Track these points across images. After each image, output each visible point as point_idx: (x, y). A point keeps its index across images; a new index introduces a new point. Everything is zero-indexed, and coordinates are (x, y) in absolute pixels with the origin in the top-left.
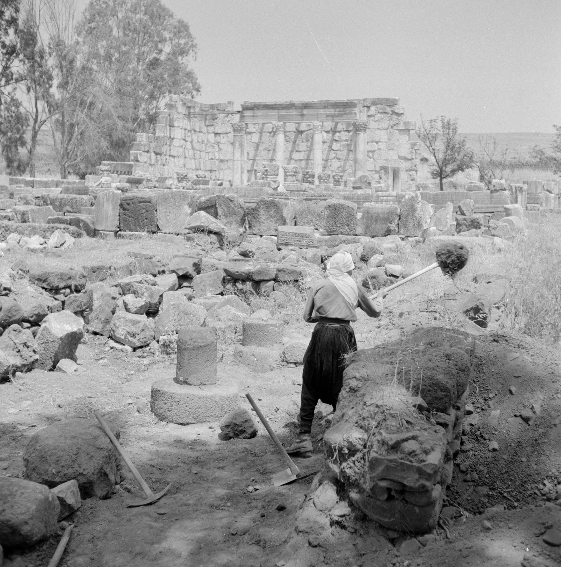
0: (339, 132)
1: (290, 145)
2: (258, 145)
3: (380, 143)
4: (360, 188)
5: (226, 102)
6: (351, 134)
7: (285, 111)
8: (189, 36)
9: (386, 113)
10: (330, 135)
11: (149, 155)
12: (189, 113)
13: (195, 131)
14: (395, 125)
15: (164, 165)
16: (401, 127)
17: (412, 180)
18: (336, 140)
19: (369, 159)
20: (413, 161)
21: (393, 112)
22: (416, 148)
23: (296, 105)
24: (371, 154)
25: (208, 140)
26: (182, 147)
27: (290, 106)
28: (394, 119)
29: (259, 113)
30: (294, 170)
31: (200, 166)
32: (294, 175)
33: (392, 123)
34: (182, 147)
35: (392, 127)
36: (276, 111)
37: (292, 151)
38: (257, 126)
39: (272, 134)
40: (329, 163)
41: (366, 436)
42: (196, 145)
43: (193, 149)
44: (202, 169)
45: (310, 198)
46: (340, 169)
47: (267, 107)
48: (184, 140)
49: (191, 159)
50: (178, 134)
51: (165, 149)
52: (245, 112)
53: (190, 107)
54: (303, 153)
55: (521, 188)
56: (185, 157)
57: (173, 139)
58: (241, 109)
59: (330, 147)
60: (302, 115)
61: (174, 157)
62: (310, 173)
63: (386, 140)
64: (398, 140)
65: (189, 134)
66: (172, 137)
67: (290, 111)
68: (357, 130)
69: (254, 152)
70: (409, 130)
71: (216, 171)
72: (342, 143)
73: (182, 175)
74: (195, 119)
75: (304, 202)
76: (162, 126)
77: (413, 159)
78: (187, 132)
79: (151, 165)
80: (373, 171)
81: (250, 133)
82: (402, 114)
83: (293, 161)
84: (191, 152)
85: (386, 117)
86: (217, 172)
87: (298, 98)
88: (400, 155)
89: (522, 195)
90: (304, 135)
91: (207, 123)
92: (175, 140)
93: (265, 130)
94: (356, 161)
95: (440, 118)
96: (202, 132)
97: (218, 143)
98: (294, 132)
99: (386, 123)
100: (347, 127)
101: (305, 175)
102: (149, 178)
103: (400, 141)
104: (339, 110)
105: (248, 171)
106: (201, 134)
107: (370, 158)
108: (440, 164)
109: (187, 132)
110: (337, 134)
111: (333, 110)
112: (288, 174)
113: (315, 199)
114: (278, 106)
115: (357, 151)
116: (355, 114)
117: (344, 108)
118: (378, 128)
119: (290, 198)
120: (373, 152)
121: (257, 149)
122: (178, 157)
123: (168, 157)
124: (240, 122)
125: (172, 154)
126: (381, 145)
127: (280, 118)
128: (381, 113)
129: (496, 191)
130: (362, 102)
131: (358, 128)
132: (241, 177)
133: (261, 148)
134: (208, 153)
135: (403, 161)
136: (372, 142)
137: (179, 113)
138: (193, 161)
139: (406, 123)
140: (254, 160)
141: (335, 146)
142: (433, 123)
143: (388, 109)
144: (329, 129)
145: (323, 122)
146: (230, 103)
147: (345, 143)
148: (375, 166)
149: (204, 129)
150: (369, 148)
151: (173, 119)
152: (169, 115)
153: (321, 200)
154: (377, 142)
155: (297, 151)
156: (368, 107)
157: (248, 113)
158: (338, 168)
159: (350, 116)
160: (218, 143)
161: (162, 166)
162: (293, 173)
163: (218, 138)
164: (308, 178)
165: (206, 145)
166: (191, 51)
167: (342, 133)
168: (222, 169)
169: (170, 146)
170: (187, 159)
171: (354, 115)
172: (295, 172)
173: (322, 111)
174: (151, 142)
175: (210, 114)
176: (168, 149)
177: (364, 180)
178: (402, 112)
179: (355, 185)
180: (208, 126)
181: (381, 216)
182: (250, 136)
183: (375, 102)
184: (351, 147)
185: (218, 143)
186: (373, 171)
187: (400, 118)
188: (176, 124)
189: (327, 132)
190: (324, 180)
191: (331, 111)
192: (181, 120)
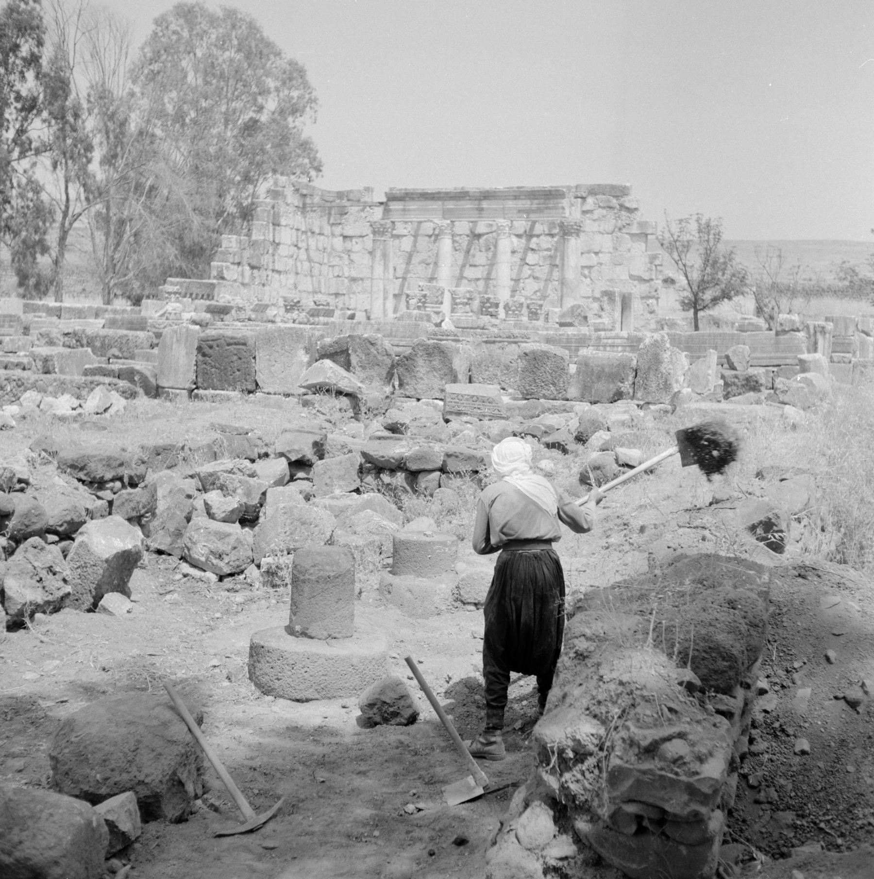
0: (538, 236)
1: (460, 256)
2: (410, 256)
3: (600, 255)
4: (570, 325)
5: (361, 188)
6: (555, 239)
7: (452, 202)
8: (306, 85)
9: (610, 208)
10: (523, 241)
11: (240, 269)
12: (304, 205)
13: (313, 233)
14: (624, 227)
15: (264, 285)
16: (635, 230)
17: (651, 312)
18: (532, 250)
19: (584, 279)
20: (652, 283)
21: (622, 206)
22: (657, 262)
23: (471, 194)
24: (586, 272)
25: (332, 246)
26: (292, 256)
27: (461, 195)
28: (624, 218)
29: (413, 205)
30: (468, 295)
31: (320, 287)
32: (467, 304)
33: (620, 223)
34: (292, 256)
35: (620, 229)
36: (440, 203)
37: (464, 266)
38: (409, 227)
39: (433, 238)
40: (521, 285)
41: (602, 731)
43: (309, 260)
44: (323, 291)
45: (493, 339)
46: (538, 294)
47: (426, 196)
48: (296, 246)
49: (306, 276)
50: (286, 236)
51: (266, 260)
52: (390, 203)
53: (305, 196)
54: (481, 268)
55: (823, 328)
56: (297, 274)
57: (278, 244)
58: (384, 200)
59: (523, 259)
60: (481, 210)
61: (279, 272)
62: (491, 301)
63: (611, 250)
64: (629, 250)
65: (304, 237)
66: (277, 241)
67: (460, 203)
68: (565, 234)
69: (404, 266)
70: (646, 235)
71: (344, 294)
72: (541, 254)
73: (292, 301)
74: (314, 214)
75: (484, 345)
76: (262, 225)
77: (652, 280)
78: (300, 233)
79: (243, 284)
80: (589, 298)
81: (398, 237)
82: (636, 209)
83: (465, 281)
84: (306, 265)
85: (611, 214)
86: (346, 297)
87: (474, 183)
88: (633, 273)
89: (824, 338)
90: (482, 240)
91: (332, 221)
92: (281, 246)
93: (421, 232)
94: (563, 282)
95: (695, 217)
96: (323, 234)
97: (349, 252)
98: (468, 236)
99: (610, 225)
100: (550, 229)
101: (484, 303)
102: (241, 306)
103: (633, 251)
104: (536, 202)
105: (395, 296)
106: (322, 238)
107: (586, 277)
108: (695, 288)
109: (300, 233)
110: (534, 240)
111: (529, 202)
112: (458, 301)
113: (500, 342)
114: (442, 195)
115: (566, 267)
116: (563, 208)
117: (545, 200)
118: (597, 230)
119: (461, 339)
120: (590, 267)
121: (408, 263)
122: (286, 272)
123: (270, 273)
124: (383, 219)
125: (276, 268)
126: (604, 258)
127: (446, 213)
128: (604, 208)
129: (785, 332)
130: (574, 190)
131: (567, 231)
132: (384, 305)
133: (415, 260)
134: (333, 266)
135: (636, 282)
136: (589, 252)
137: (288, 205)
138: (309, 278)
139: (642, 225)
140: (404, 279)
141: (531, 258)
142: (684, 224)
143: (614, 202)
144: (521, 232)
145: (512, 221)
146: (368, 189)
147: (546, 253)
148: (593, 291)
149: (327, 230)
150: (584, 261)
151: (279, 213)
152: (273, 207)
153: (510, 343)
154: (596, 253)
155: (471, 266)
156: (584, 198)
157: (395, 206)
158: (535, 292)
159: (554, 211)
160: (349, 251)
161: (261, 287)
162: (466, 300)
163: (348, 244)
164: (489, 307)
165: (330, 255)
166: (308, 109)
167: (542, 237)
168: (354, 293)
169: (273, 255)
170: (299, 276)
171: (561, 211)
172: (470, 299)
173: (510, 204)
174: (244, 249)
175: (337, 206)
176: (271, 260)
177: (577, 313)
178: (634, 206)
179: (563, 321)
180: (333, 224)
181: (607, 370)
182: (397, 241)
183: (593, 191)
184: (556, 261)
185: (349, 252)
186: (589, 298)
187: (633, 215)
188: (283, 222)
189: (519, 236)
190: (514, 311)
191: (526, 204)
192: (291, 215)
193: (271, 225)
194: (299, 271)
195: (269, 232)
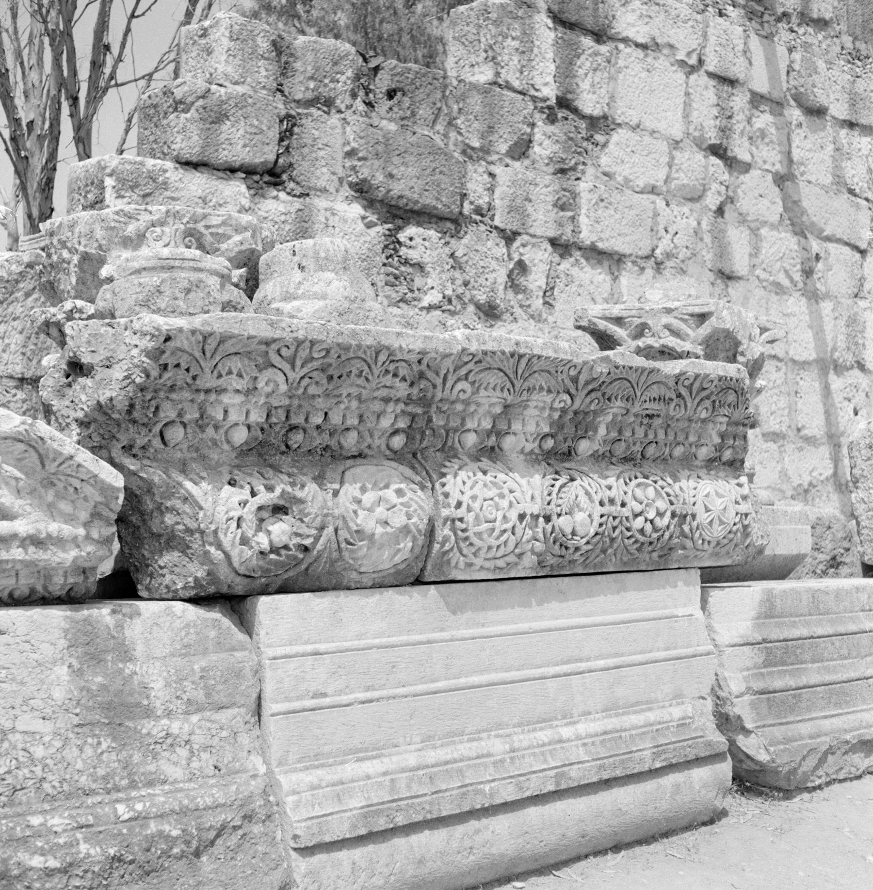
13: (817, 112)
26: (695, 198)
34: (695, 198)
42: (814, 202)
43: (796, 222)
48: (718, 151)
49: (779, 289)
56: (727, 277)
57: (601, 124)
61: (596, 254)
65: (764, 120)
78: (739, 101)
84: (781, 245)
109: (739, 101)
123: (539, 257)
125: (587, 236)
138: (796, 304)
170: (736, 290)
193: (542, 20)
194: (740, 263)
195: (526, 50)
